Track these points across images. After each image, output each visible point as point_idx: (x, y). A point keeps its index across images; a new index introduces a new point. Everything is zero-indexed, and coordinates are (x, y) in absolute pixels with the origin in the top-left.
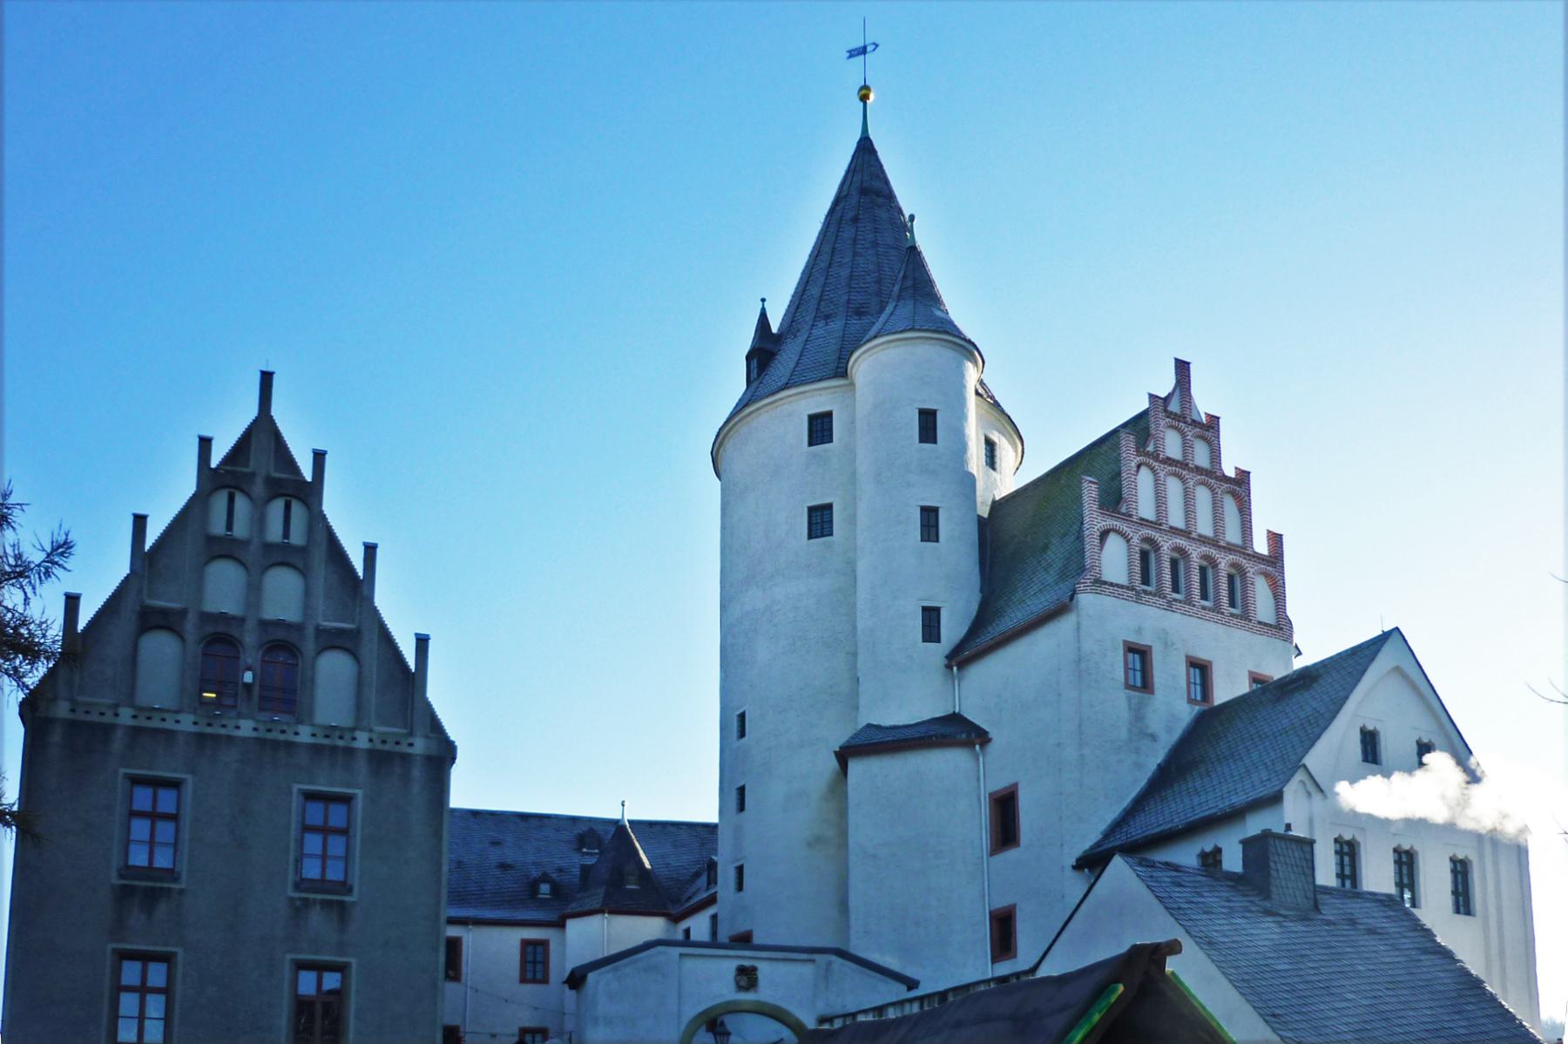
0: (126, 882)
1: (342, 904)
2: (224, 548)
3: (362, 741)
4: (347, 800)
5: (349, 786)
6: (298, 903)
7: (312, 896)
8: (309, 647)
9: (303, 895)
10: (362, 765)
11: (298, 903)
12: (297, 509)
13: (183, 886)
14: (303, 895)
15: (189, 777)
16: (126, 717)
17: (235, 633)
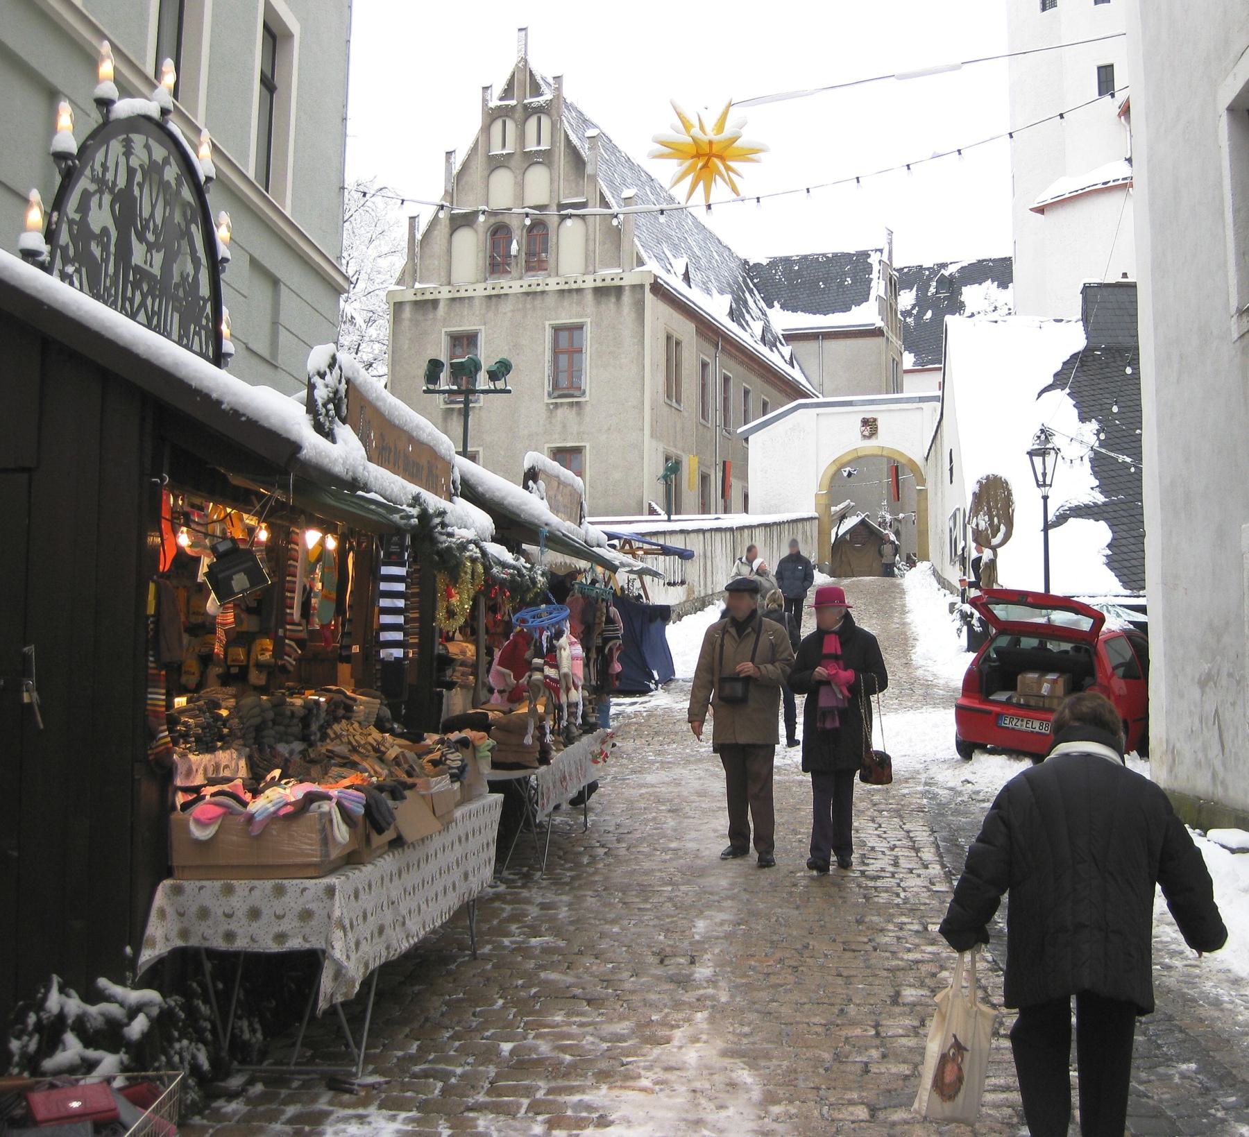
0: (449, 406)
1: (577, 403)
2: (496, 163)
3: (590, 284)
4: (580, 327)
5: (581, 317)
6: (551, 407)
7: (559, 401)
8: (553, 221)
9: (554, 401)
10: (589, 297)
11: (551, 407)
12: (545, 121)
13: (481, 404)
14: (554, 401)
15: (482, 328)
16: (445, 294)
17: (506, 219)
